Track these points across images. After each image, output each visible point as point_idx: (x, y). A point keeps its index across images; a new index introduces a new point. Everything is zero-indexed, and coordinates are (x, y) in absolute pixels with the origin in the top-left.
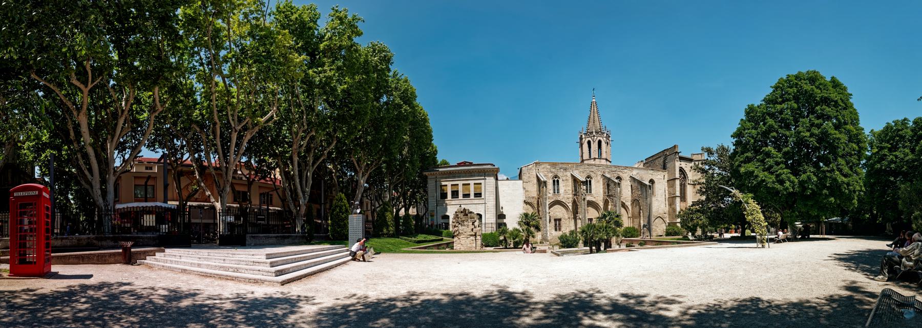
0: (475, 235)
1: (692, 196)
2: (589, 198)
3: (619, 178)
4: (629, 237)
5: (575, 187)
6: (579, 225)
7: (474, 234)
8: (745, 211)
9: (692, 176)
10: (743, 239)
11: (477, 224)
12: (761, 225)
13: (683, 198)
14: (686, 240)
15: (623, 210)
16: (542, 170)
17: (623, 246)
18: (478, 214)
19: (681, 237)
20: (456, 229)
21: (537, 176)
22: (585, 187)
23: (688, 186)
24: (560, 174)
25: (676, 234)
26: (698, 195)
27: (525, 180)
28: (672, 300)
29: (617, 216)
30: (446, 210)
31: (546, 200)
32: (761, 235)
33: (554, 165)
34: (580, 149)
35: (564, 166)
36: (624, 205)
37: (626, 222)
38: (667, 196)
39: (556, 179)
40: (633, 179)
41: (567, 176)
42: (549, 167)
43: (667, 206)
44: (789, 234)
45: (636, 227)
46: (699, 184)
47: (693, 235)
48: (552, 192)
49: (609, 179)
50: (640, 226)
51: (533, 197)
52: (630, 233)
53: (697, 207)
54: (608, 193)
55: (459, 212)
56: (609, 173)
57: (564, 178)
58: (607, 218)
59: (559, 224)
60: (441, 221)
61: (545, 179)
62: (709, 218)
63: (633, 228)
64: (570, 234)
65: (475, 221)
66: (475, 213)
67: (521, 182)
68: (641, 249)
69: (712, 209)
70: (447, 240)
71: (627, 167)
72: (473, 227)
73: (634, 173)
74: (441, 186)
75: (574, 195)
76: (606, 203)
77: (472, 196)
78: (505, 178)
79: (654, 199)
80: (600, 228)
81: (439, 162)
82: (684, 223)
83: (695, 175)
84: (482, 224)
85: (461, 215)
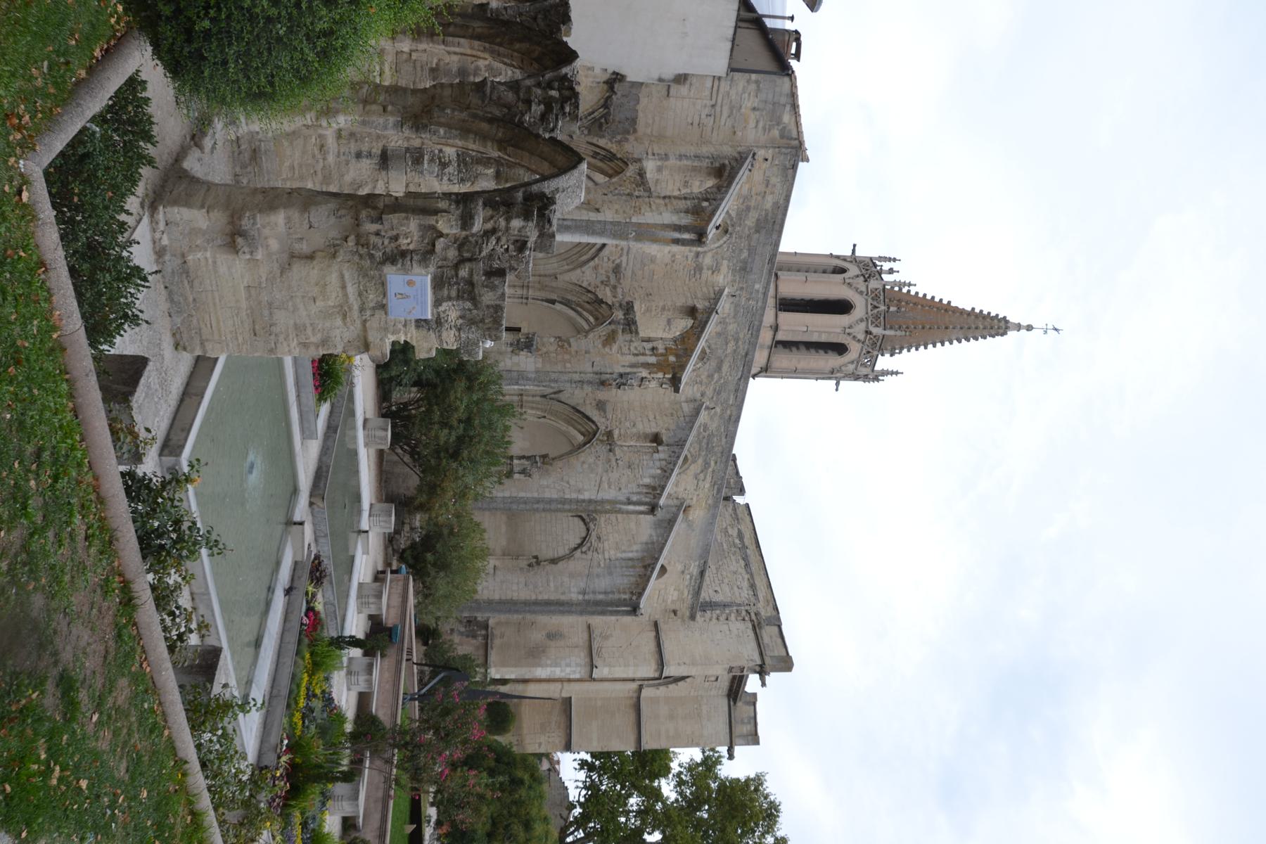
41: (715, 270)
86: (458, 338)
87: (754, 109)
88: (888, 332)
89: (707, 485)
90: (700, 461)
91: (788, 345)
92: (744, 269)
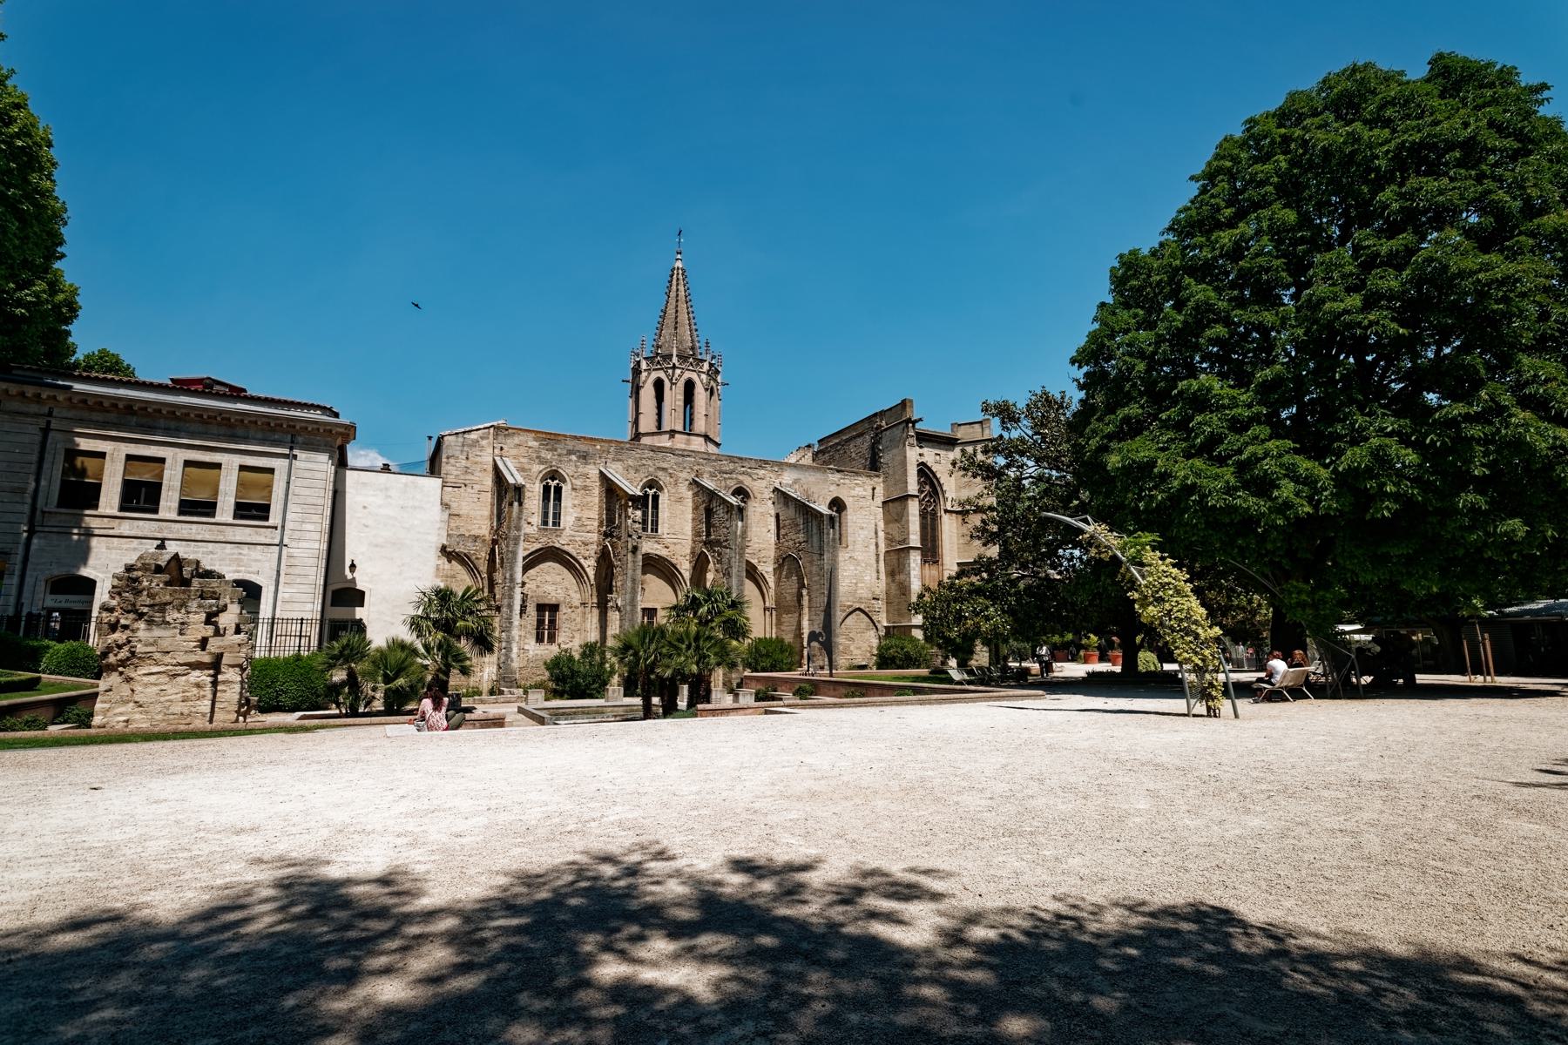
0: (216, 665)
1: (956, 545)
2: (648, 547)
3: (741, 492)
4: (764, 670)
5: (610, 511)
6: (614, 628)
7: (207, 659)
8: (1131, 589)
9: (955, 488)
10: (1131, 682)
11: (228, 619)
12: (1197, 636)
13: (931, 552)
14: (941, 681)
15: (749, 587)
16: (514, 452)
17: (747, 699)
18: (239, 583)
19: (924, 672)
20: (119, 636)
21: (496, 468)
22: (639, 513)
23: (946, 518)
24: (566, 470)
25: (909, 661)
26: (977, 543)
27: (451, 479)
28: (910, 886)
29: (734, 605)
30: (83, 554)
31: (516, 544)
32: (1199, 670)
33: (550, 439)
34: (631, 402)
35: (582, 447)
36: (752, 573)
37: (759, 624)
38: (882, 549)
39: (553, 484)
40: (782, 497)
41: (586, 476)
42: (535, 444)
43: (883, 576)
44: (1315, 668)
45: (788, 638)
46: (979, 510)
47: (962, 665)
48: (536, 519)
49: (712, 495)
50: (799, 635)
51: (475, 538)
52: (767, 655)
53: (974, 579)
54: (708, 534)
55: (145, 568)
56: (712, 475)
57: (578, 483)
58: (703, 610)
59: (552, 622)
60: (40, 599)
61: (521, 481)
62: (1011, 612)
63: (780, 641)
64: (583, 655)
65: (224, 609)
66: (230, 577)
67: (435, 483)
68: (804, 707)
69: (1022, 585)
70: (56, 684)
71: (766, 462)
72: (210, 630)
73: (787, 480)
74: (73, 453)
75: (606, 535)
76: (700, 565)
77: (225, 511)
78: (380, 463)
79: (843, 556)
80: (681, 640)
81: (80, 355)
82: (934, 631)
83: (968, 485)
84: (255, 621)
85: (155, 583)
86: (196, 613)
87: (467, 458)
88: (675, 353)
89: (763, 472)
90: (741, 477)
92: (585, 458)
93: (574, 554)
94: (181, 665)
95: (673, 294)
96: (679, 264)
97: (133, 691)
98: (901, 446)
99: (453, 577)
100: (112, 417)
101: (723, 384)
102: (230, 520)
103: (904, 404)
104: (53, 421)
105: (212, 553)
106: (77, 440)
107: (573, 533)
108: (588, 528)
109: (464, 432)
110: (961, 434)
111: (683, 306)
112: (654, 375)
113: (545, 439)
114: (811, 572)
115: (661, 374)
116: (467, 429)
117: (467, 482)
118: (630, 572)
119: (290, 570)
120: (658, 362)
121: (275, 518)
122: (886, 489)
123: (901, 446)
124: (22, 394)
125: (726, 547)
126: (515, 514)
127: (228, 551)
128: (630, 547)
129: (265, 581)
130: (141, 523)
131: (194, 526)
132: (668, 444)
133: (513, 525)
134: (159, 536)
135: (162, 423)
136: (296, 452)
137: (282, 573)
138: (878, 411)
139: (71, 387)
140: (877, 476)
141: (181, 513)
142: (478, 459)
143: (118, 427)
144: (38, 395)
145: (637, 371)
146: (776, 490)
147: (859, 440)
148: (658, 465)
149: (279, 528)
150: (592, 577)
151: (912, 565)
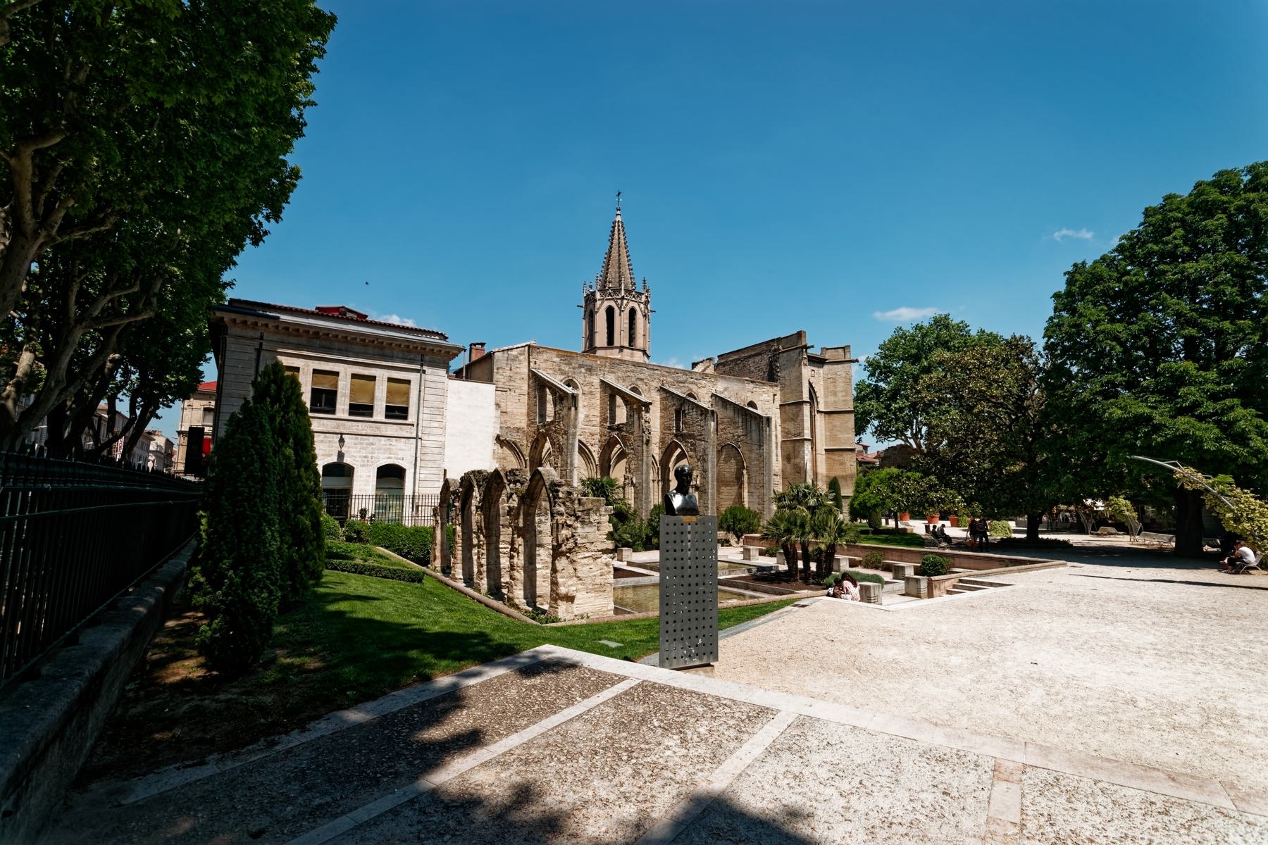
24: (579, 380)
41: (591, 384)
42: (557, 360)
51: (518, 429)
57: (586, 389)
77: (379, 413)
90: (691, 386)
91: (632, 338)
93: (585, 442)
94: (599, 551)
95: (615, 241)
96: (619, 218)
97: (575, 569)
98: (797, 366)
99: (505, 459)
100: (303, 340)
101: (651, 311)
102: (346, 416)
103: (800, 335)
104: (264, 343)
105: (372, 444)
106: (280, 358)
107: (584, 426)
108: (594, 423)
109: (508, 350)
110: (828, 356)
111: (623, 251)
112: (606, 304)
113: (563, 356)
114: (750, 458)
115: (612, 303)
116: (510, 347)
117: (511, 387)
118: (645, 459)
119: (423, 457)
120: (610, 294)
121: (412, 418)
122: (783, 395)
123: (797, 366)
124: (245, 322)
125: (700, 440)
126: (572, 416)
127: (383, 443)
128: (645, 440)
129: (407, 464)
130: (325, 421)
131: (360, 424)
132: (619, 357)
133: (571, 424)
134: (338, 431)
135: (336, 345)
136: (425, 368)
137: (418, 459)
138: (775, 337)
139: (278, 318)
140: (777, 386)
141: (350, 414)
142: (518, 370)
143: (308, 348)
144: (256, 324)
145: (590, 299)
146: (713, 395)
147: (757, 359)
148: (638, 376)
149: (415, 425)
150: (597, 459)
151: (806, 452)
